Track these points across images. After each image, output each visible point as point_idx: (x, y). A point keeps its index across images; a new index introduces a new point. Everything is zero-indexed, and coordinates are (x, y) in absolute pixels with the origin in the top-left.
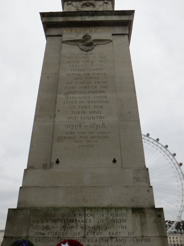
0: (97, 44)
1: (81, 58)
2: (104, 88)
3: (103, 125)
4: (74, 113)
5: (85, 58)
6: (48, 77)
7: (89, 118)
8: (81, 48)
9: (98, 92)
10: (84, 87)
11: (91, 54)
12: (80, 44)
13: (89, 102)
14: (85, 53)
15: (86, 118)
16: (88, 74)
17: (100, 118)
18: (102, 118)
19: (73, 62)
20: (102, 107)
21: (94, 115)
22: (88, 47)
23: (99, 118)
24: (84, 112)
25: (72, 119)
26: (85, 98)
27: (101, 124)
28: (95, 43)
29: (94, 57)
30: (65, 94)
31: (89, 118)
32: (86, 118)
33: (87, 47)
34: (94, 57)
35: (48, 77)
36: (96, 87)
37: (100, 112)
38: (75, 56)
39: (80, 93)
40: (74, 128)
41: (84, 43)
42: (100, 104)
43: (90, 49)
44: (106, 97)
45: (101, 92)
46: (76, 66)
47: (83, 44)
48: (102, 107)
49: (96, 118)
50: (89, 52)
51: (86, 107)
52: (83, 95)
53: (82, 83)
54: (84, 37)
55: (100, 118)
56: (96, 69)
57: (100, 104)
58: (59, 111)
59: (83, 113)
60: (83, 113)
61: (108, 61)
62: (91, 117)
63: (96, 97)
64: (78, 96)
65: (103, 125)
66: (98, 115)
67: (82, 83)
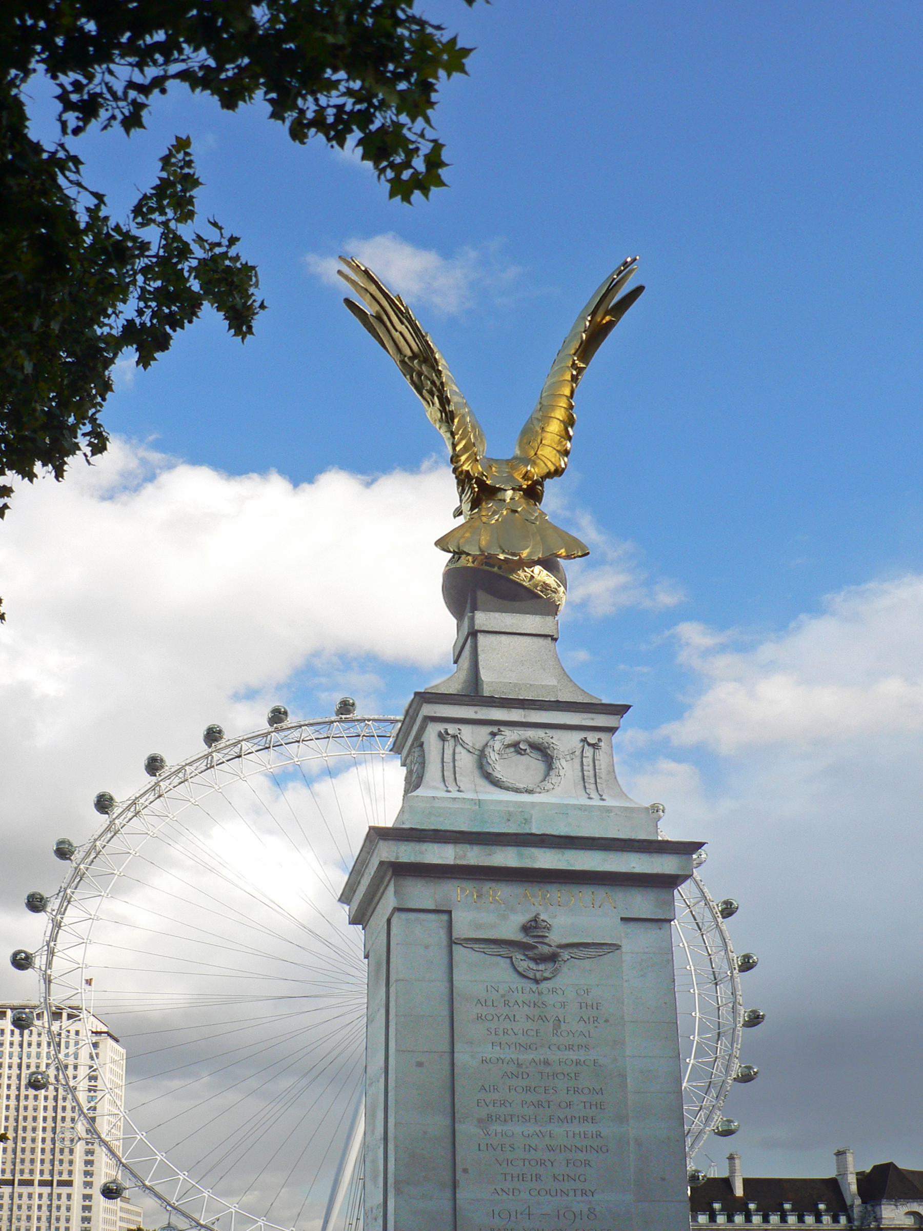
0: (572, 957)
1: (520, 1004)
2: (594, 1108)
3: (592, 1211)
4: (508, 1177)
5: (535, 1004)
6: (420, 1064)
7: (553, 1193)
8: (520, 969)
9: (578, 1119)
10: (536, 1103)
11: (554, 991)
12: (518, 956)
13: (551, 1149)
14: (534, 987)
15: (543, 1193)
16: (547, 1063)
17: (584, 1193)
18: (589, 1193)
19: (496, 1017)
20: (587, 1163)
21: (566, 1186)
22: (542, 967)
23: (579, 1193)
24: (538, 1177)
25: (504, 1194)
26: (541, 1136)
27: (585, 1210)
28: (565, 955)
29: (563, 1005)
30: (480, 1121)
31: (553, 1193)
32: (543, 1193)
33: (537, 964)
34: (563, 1005)
35: (420, 1064)
36: (569, 1105)
37: (582, 1178)
38: (503, 996)
39: (525, 1119)
40: (513, 1219)
41: (530, 954)
42: (581, 1156)
43: (546, 975)
44: (599, 1135)
45: (585, 1119)
46: (505, 1032)
47: (526, 956)
48: (587, 1163)
49: (571, 1193)
50: (544, 985)
51: (542, 1163)
52: (531, 1128)
53: (528, 1089)
54: (526, 929)
55: (584, 1193)
56: (570, 1047)
57: (581, 1156)
58: (465, 1171)
59: (534, 1178)
60: (534, 1178)
61: (607, 1021)
62: (559, 1191)
63: (571, 1134)
64: (518, 1129)
65: (592, 1211)
66: (579, 1185)
67: (528, 1089)
